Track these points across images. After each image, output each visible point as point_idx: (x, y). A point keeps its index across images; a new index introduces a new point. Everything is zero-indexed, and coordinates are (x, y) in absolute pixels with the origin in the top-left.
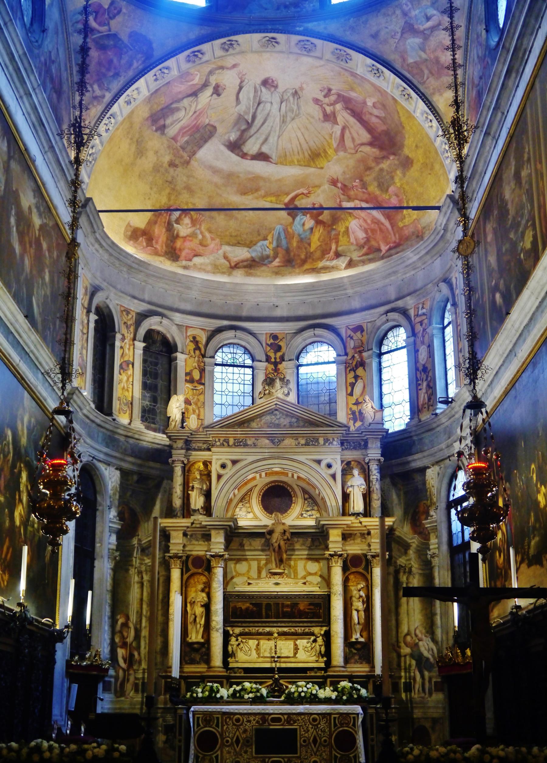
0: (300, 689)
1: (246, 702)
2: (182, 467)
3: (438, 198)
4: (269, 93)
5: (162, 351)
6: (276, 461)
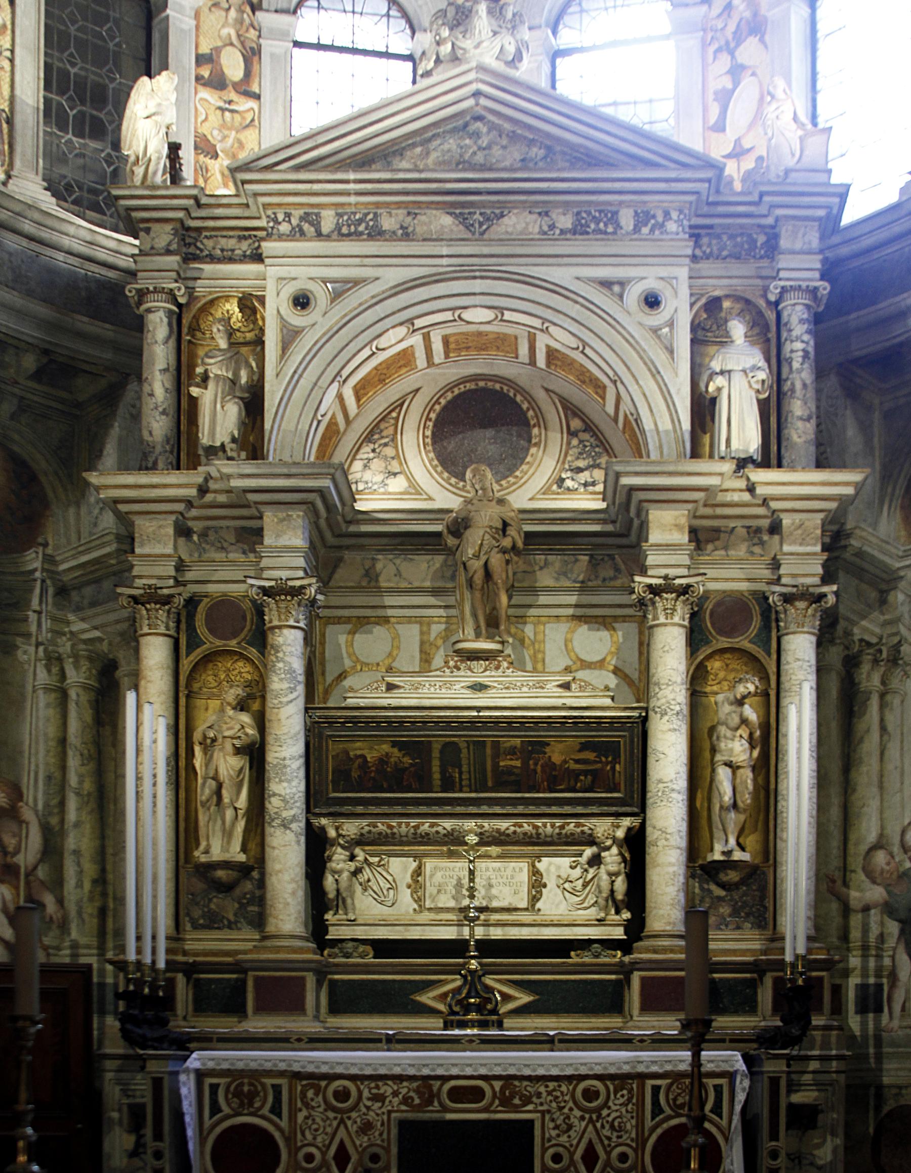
2: (170, 313)
6: (478, 285)
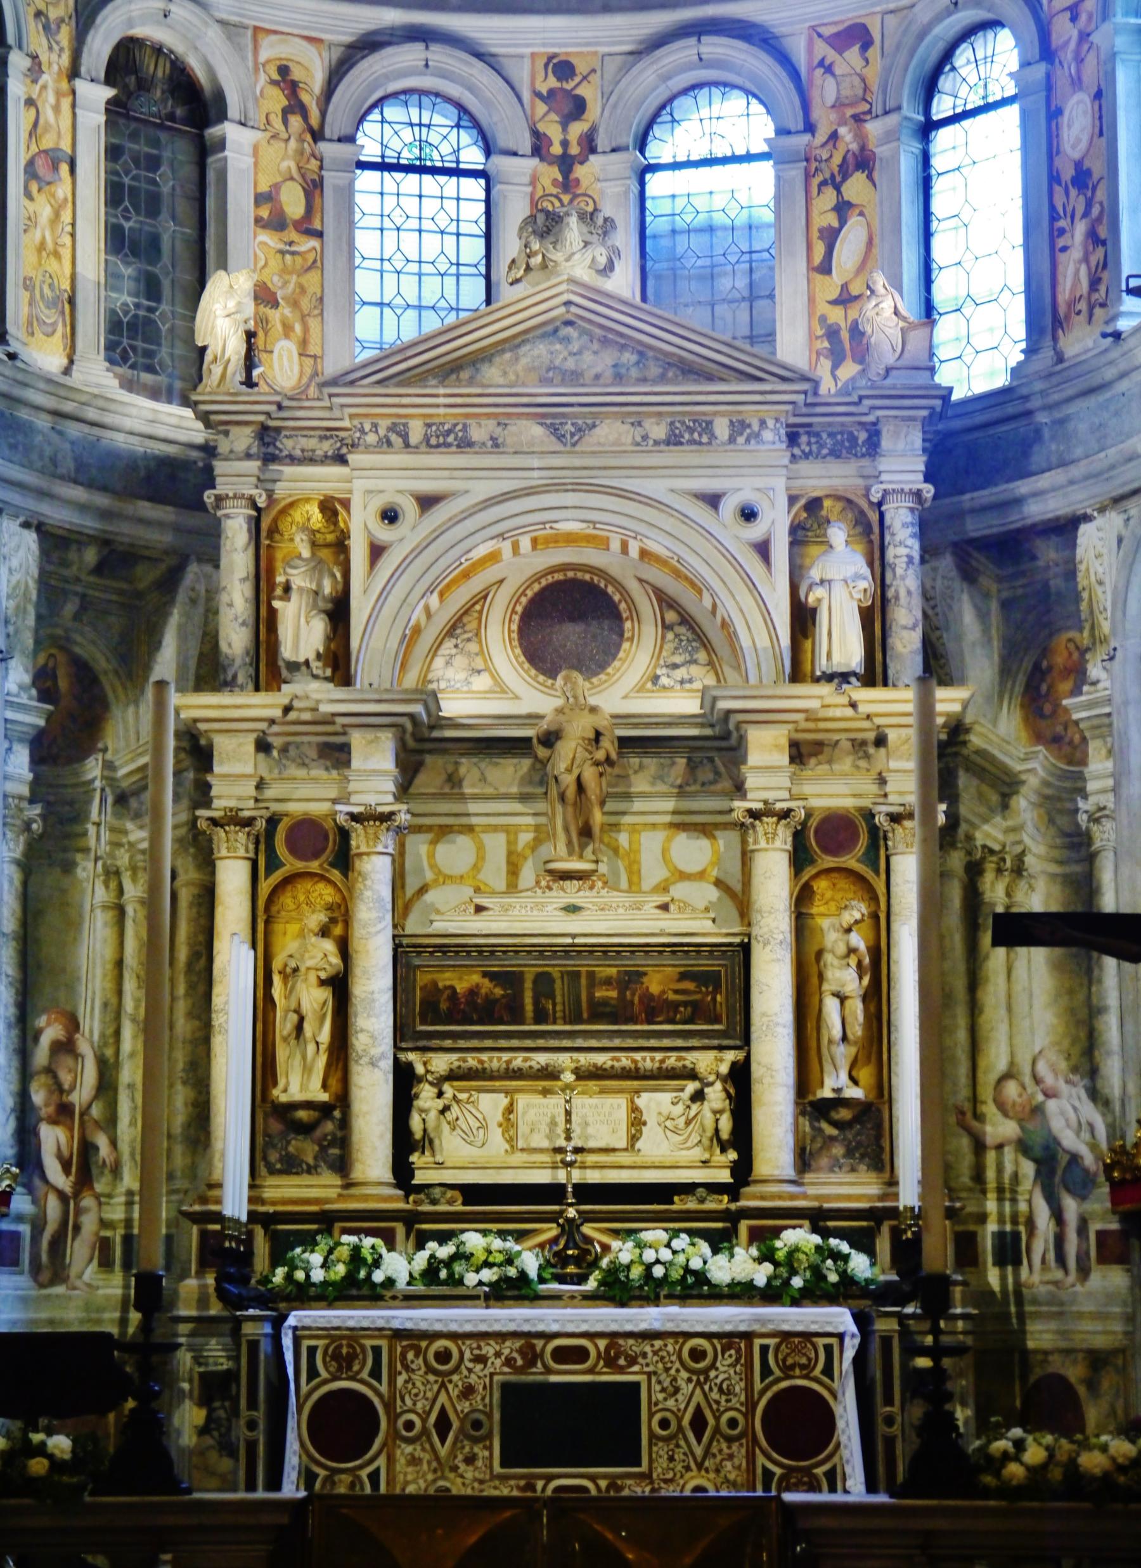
0: (649, 1256)
1: (469, 1298)
5: (172, 117)
6: (570, 499)
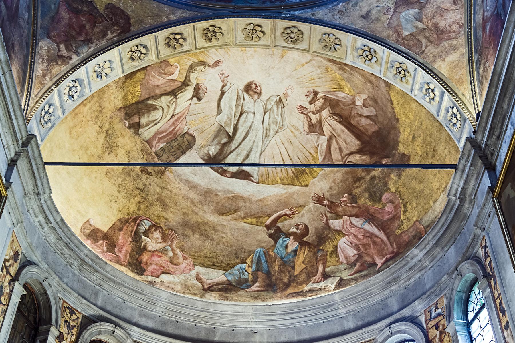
3: (444, 186)
4: (253, 101)
